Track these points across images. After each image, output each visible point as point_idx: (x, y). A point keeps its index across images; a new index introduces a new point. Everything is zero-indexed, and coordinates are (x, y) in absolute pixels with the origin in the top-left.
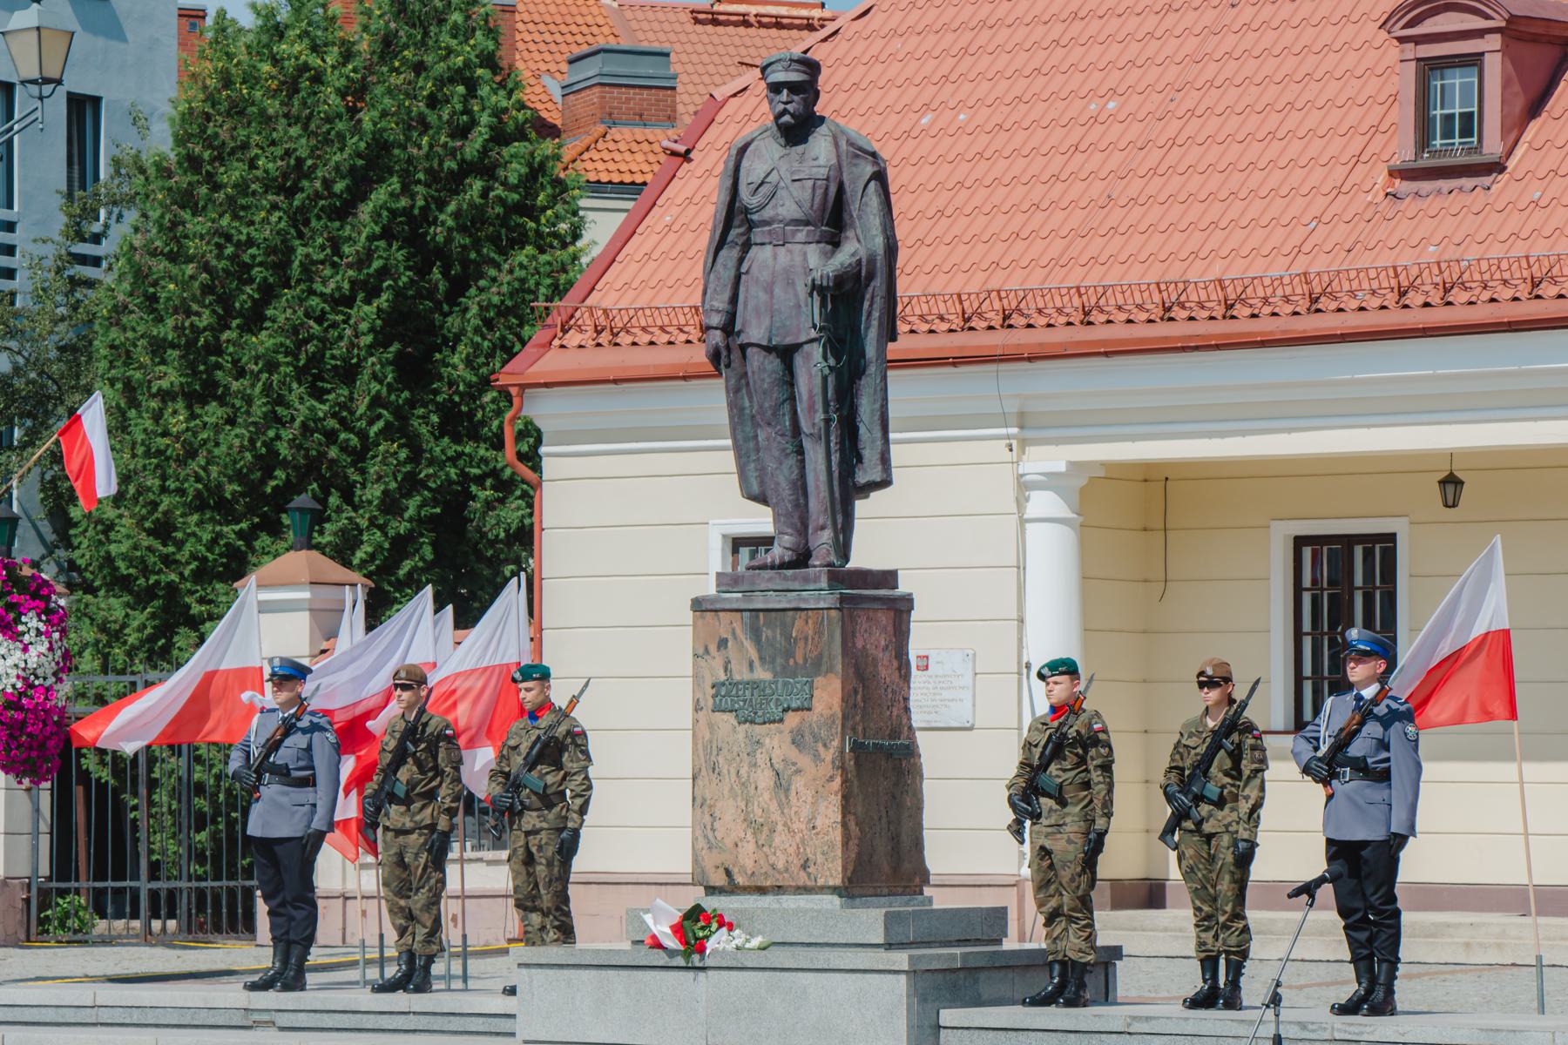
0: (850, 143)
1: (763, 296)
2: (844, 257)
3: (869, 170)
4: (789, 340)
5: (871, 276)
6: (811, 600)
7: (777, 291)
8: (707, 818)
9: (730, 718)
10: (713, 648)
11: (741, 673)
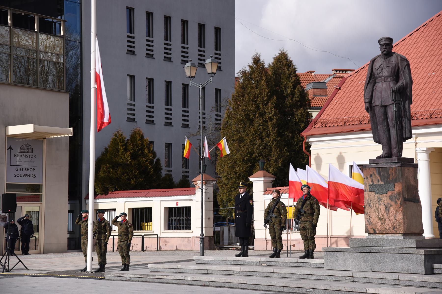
0: (401, 57)
1: (379, 94)
2: (399, 84)
3: (406, 63)
4: (386, 104)
5: (407, 88)
6: (394, 165)
7: (383, 93)
8: (368, 217)
10: (369, 177)
11: (376, 183)
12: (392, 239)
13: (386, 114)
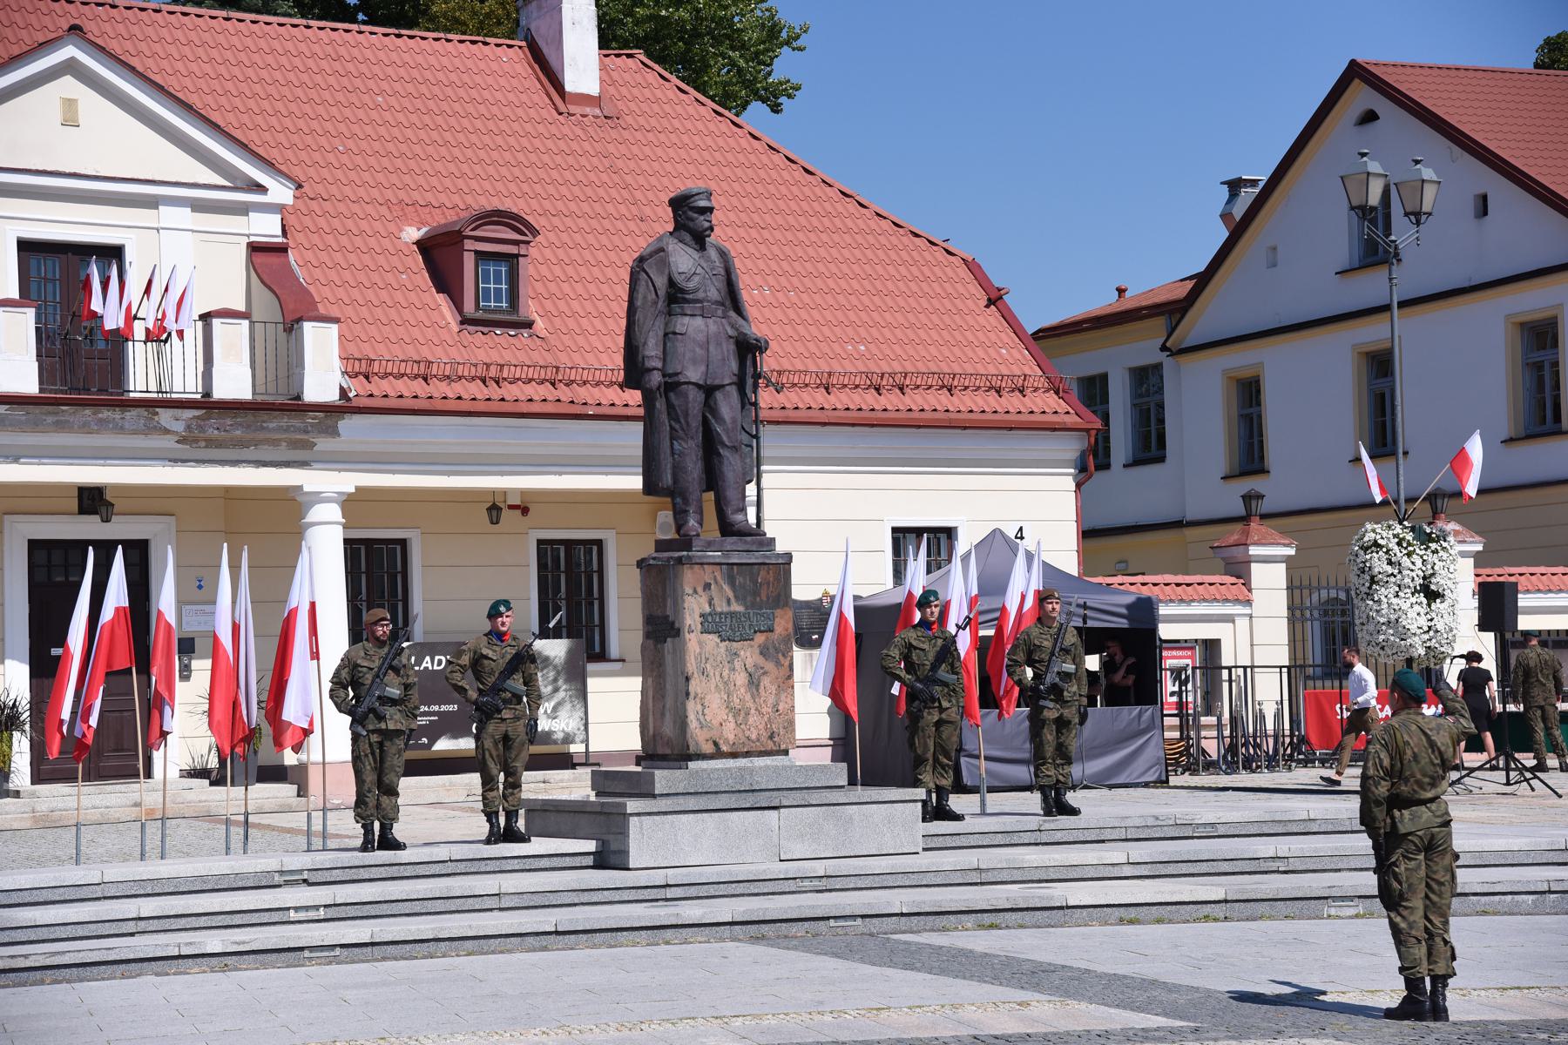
4: (717, 382)
7: (711, 348)
8: (699, 707)
9: (714, 638)
10: (700, 590)
11: (721, 607)
12: (767, 767)
13: (710, 406)
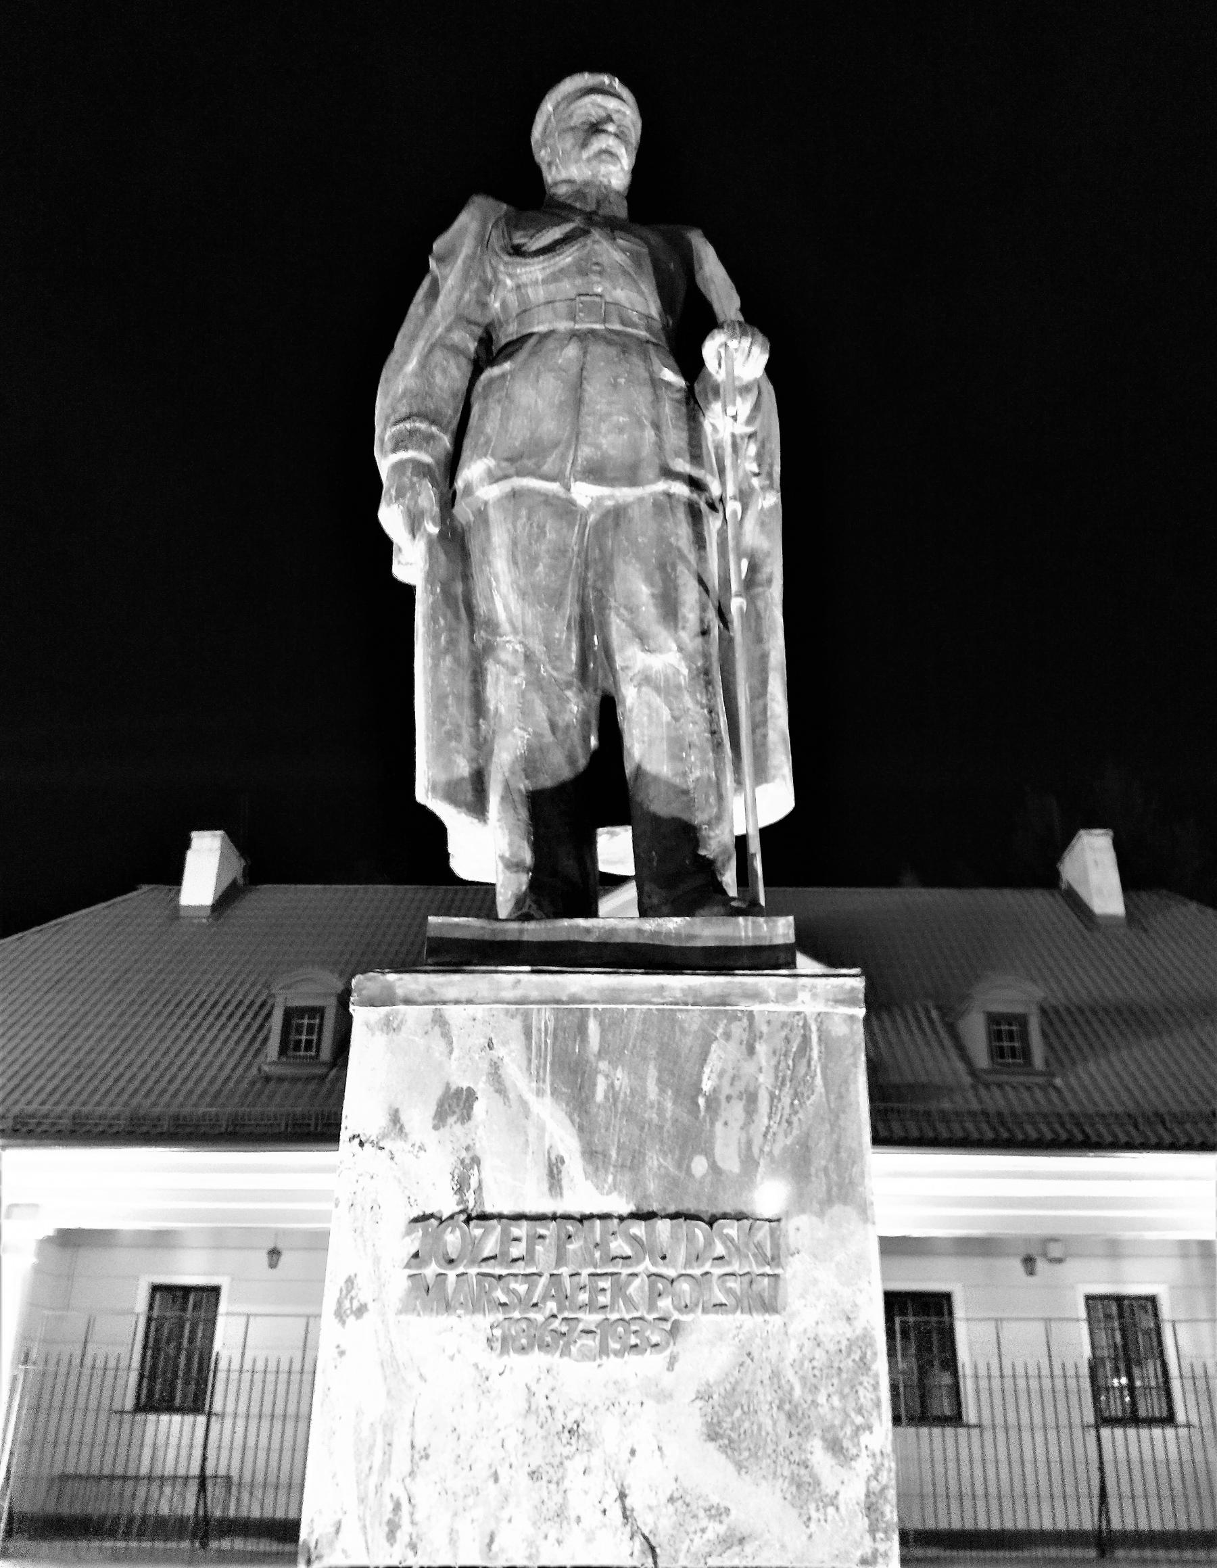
10: (418, 1118)
